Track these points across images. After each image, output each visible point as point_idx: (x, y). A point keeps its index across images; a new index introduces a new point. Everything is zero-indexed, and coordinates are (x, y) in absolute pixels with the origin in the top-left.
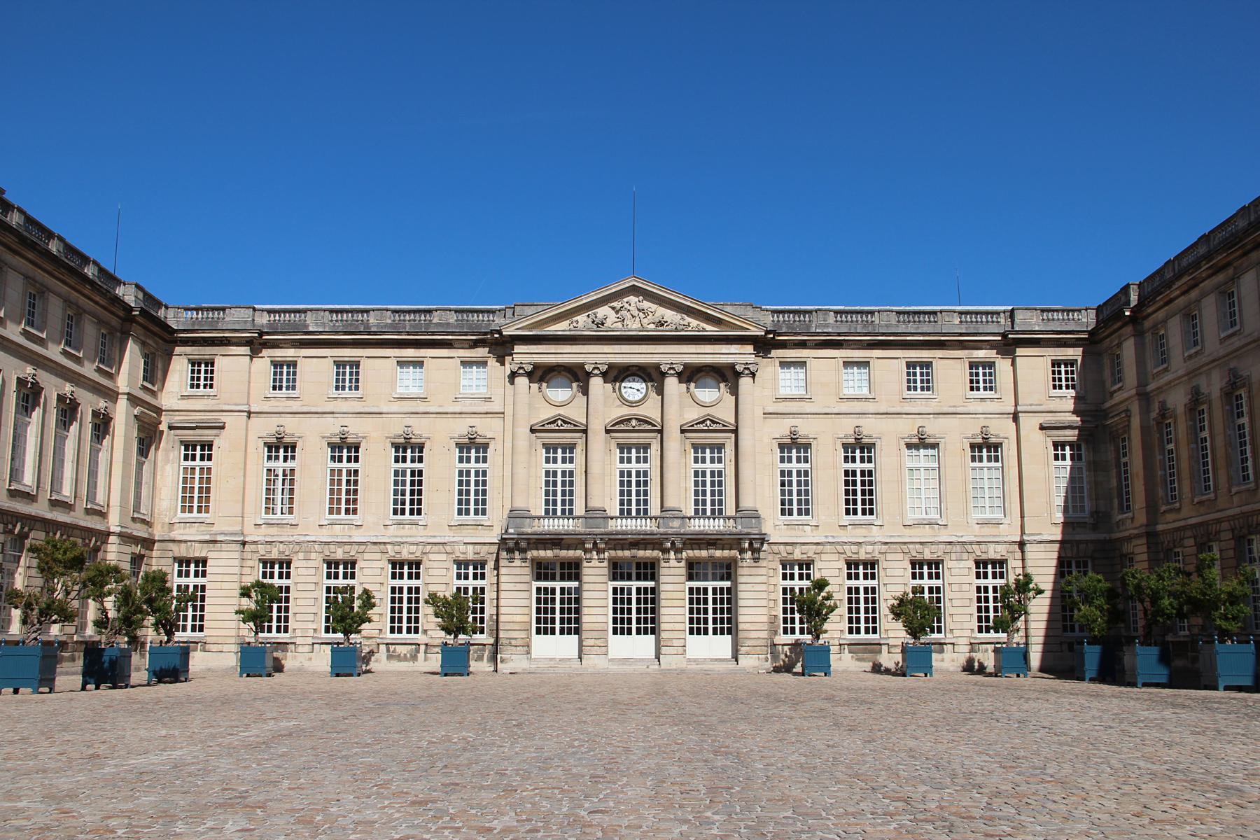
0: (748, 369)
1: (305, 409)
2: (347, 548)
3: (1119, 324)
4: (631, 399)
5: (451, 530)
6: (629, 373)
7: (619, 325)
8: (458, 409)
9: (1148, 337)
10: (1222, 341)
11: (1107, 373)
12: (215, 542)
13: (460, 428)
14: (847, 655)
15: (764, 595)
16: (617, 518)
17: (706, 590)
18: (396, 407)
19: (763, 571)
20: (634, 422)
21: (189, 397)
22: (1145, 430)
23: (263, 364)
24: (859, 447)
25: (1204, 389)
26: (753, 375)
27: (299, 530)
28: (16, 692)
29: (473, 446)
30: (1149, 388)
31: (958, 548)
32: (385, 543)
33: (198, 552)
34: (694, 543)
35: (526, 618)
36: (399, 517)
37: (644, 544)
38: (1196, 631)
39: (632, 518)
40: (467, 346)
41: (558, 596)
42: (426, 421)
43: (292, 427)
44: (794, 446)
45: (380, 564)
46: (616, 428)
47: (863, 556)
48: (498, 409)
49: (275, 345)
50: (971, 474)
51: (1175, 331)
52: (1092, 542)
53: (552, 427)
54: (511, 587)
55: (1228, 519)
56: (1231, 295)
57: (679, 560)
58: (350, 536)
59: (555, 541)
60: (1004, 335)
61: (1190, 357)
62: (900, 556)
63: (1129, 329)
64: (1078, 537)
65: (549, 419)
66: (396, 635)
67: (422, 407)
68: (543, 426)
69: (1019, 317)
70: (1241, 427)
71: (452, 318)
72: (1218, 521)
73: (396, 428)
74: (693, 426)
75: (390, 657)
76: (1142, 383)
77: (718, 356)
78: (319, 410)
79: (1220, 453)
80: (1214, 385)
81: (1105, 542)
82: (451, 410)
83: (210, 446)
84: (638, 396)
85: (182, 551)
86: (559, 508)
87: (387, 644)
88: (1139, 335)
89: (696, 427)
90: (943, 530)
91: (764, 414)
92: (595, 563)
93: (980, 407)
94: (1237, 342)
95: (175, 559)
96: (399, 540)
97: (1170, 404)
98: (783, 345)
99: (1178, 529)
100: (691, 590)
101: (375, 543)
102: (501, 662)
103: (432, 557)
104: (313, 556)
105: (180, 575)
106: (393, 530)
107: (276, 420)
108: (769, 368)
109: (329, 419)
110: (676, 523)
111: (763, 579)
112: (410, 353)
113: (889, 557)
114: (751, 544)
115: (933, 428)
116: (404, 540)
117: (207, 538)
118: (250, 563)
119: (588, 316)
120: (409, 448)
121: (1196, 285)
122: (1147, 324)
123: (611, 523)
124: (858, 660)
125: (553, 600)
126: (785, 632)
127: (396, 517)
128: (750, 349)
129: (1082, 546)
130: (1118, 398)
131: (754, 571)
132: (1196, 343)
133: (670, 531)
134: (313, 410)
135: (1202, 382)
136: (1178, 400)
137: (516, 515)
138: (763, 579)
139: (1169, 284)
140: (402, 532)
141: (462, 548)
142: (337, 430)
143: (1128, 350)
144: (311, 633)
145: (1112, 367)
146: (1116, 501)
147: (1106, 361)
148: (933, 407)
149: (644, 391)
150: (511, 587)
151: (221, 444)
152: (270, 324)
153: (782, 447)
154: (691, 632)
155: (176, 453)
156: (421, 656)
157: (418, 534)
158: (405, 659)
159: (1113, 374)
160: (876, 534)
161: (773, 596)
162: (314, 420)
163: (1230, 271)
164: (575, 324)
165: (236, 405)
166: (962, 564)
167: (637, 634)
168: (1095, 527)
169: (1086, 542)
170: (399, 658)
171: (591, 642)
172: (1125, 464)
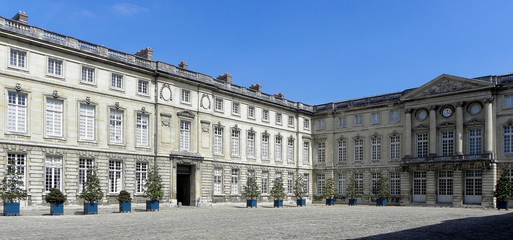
0: (489, 100)
1: (348, 130)
4: (446, 116)
5: (388, 163)
6: (445, 107)
8: (390, 126)
13: (391, 131)
16: (442, 156)
18: (371, 128)
23: (337, 119)
27: (347, 165)
29: (394, 136)
32: (370, 168)
34: (465, 164)
36: (374, 160)
37: (447, 165)
39: (447, 156)
40: (392, 106)
42: (381, 130)
43: (345, 135)
45: (369, 174)
48: (401, 124)
49: (339, 113)
58: (360, 166)
59: (418, 165)
65: (418, 126)
68: (416, 128)
74: (468, 123)
77: (477, 97)
78: (351, 130)
82: (388, 126)
84: (449, 115)
86: (423, 154)
89: (469, 124)
91: (497, 116)
96: (374, 167)
101: (367, 168)
103: (383, 171)
104: (351, 172)
105: (319, 179)
106: (372, 164)
107: (340, 135)
110: (457, 158)
116: (375, 166)
117: (324, 168)
119: (429, 90)
127: (373, 160)
134: (350, 130)
137: (406, 158)
140: (375, 164)
142: (356, 136)
149: (451, 113)
153: (505, 128)
155: (316, 146)
164: (424, 94)
165: (330, 131)
167: (447, 194)
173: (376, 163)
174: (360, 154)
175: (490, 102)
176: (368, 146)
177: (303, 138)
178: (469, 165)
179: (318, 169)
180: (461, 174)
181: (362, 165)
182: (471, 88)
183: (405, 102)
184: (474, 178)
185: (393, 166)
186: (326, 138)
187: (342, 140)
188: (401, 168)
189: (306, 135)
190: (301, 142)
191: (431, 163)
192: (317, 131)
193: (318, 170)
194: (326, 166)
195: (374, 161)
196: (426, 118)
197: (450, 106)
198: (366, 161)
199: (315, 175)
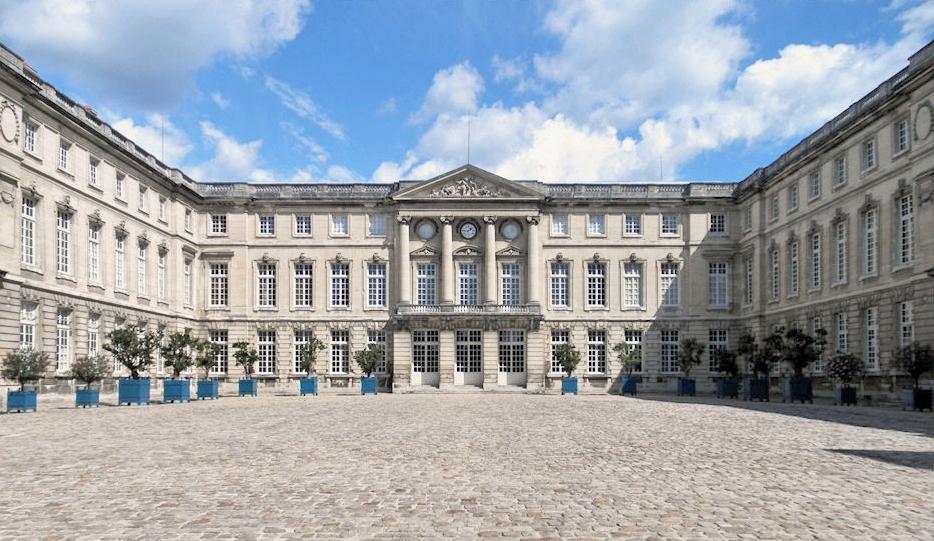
3: (750, 194)
7: (459, 195)
9: (768, 201)
10: (810, 203)
11: (742, 222)
12: (231, 321)
14: (588, 383)
15: (541, 350)
17: (509, 347)
19: (541, 336)
20: (469, 251)
21: (212, 237)
22: (762, 255)
24: (597, 265)
25: (796, 233)
26: (537, 223)
28: (129, 404)
30: (766, 231)
32: (328, 321)
33: (221, 326)
35: (408, 363)
36: (336, 305)
38: (784, 371)
41: (426, 350)
42: (349, 250)
44: (559, 264)
46: (459, 254)
47: (598, 328)
49: (261, 206)
50: (660, 281)
51: (783, 196)
53: (422, 253)
54: (399, 345)
55: (805, 308)
56: (842, 161)
57: (494, 329)
59: (424, 318)
60: (684, 200)
61: (791, 213)
62: (619, 328)
63: (757, 196)
64: (720, 318)
66: (336, 373)
67: (347, 242)
69: (694, 189)
70: (816, 255)
71: (364, 190)
72: (800, 309)
73: (332, 254)
75: (332, 385)
76: (762, 228)
79: (803, 269)
80: (802, 230)
81: (736, 321)
83: (226, 266)
85: (213, 326)
87: (331, 379)
88: (762, 199)
93: (667, 242)
94: (817, 205)
95: (209, 330)
97: (777, 242)
98: (555, 205)
99: (776, 314)
102: (396, 386)
107: (263, 251)
108: (545, 220)
109: (295, 250)
110: (493, 309)
111: (541, 340)
112: (339, 209)
114: (534, 321)
115: (640, 254)
117: (227, 318)
118: (252, 333)
120: (340, 266)
121: (797, 170)
122: (768, 193)
124: (595, 386)
125: (423, 352)
126: (554, 370)
128: (535, 208)
129: (723, 323)
130: (748, 237)
131: (536, 336)
132: (795, 205)
133: (490, 313)
135: (796, 228)
136: (782, 239)
138: (541, 340)
139: (781, 170)
141: (372, 324)
143: (756, 208)
144: (288, 372)
145: (746, 218)
146: (744, 297)
147: (743, 215)
148: (640, 242)
150: (399, 345)
151: (232, 264)
152: (258, 194)
156: (350, 384)
157: (348, 316)
158: (341, 386)
159: (746, 223)
160: (606, 316)
161: (547, 350)
162: (287, 250)
163: (817, 162)
168: (731, 312)
169: (725, 320)
170: (338, 386)
172: (750, 276)
173: (340, 313)
174: (307, 294)
175: (537, 223)
176: (323, 278)
177: (183, 249)
178: (508, 322)
179: (211, 319)
182: (509, 196)
183: (399, 202)
184: (512, 344)
185: (375, 319)
186: (230, 255)
187: (267, 266)
188: (395, 322)
189: (187, 244)
190: (180, 257)
192: (209, 237)
194: (231, 313)
195: (337, 310)
196: (434, 236)
197: (472, 221)
199: (203, 332)
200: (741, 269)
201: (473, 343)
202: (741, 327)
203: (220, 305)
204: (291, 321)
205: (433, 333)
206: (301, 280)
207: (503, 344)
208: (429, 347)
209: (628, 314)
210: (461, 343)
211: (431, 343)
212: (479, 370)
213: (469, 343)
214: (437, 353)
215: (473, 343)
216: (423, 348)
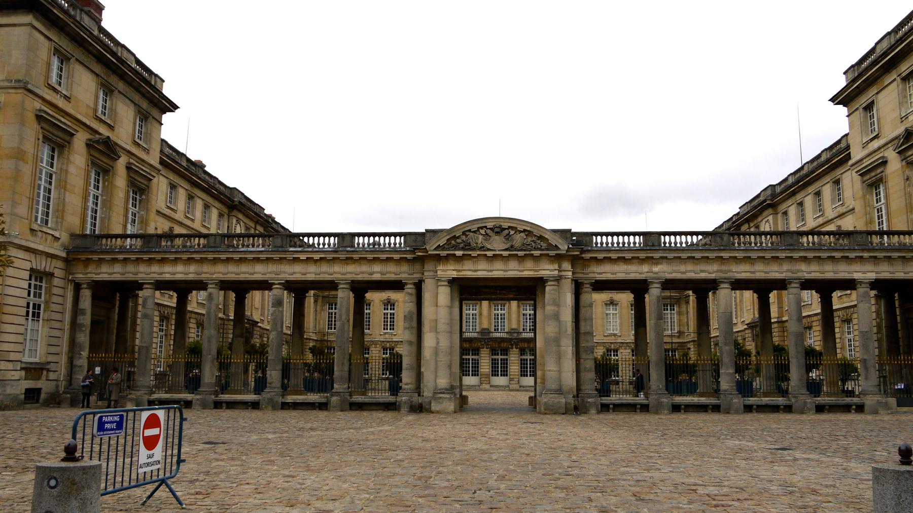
2: (391, 343)
27: (372, 337)
31: (625, 345)
52: (677, 343)
57: (516, 348)
62: (602, 348)
90: (619, 338)
92: (485, 349)
100: (521, 360)
104: (378, 346)
110: (516, 335)
113: (598, 348)
123: (491, 334)
142: (386, 298)
154: (521, 376)
166: (626, 351)
168: (679, 337)
171: (483, 379)
180: (518, 353)
181: (393, 337)
191: (488, 338)
193: (327, 341)
198: (400, 332)
200: (684, 308)
201: (503, 357)
202: (686, 348)
203: (333, 330)
204: (381, 341)
205: (475, 350)
206: (387, 314)
207: (523, 357)
208: (472, 359)
209: (608, 338)
210: (494, 357)
211: (474, 357)
212: (507, 376)
213: (500, 357)
214: (478, 363)
215: (503, 357)
216: (469, 359)
